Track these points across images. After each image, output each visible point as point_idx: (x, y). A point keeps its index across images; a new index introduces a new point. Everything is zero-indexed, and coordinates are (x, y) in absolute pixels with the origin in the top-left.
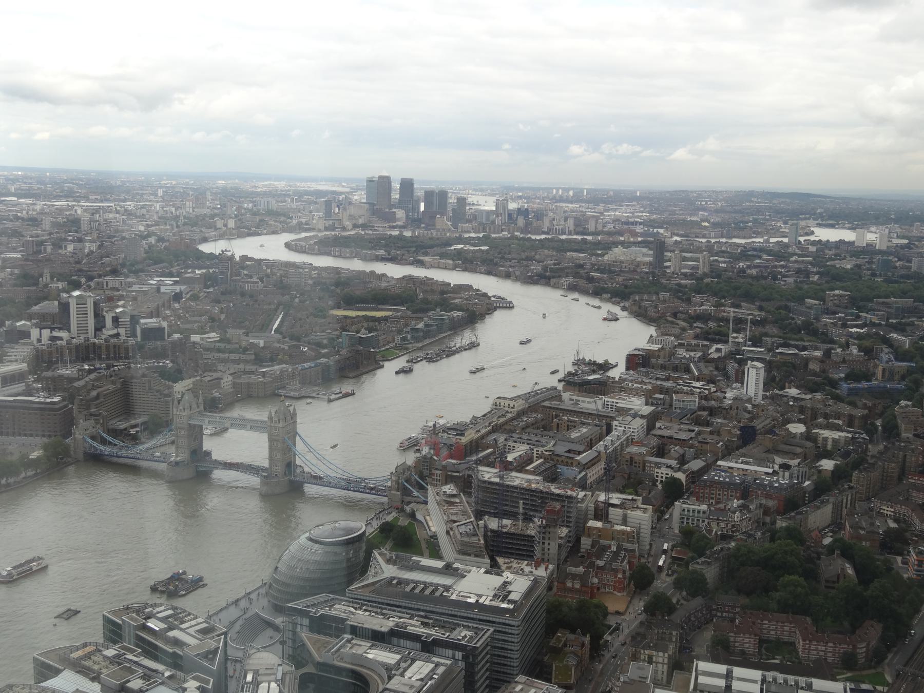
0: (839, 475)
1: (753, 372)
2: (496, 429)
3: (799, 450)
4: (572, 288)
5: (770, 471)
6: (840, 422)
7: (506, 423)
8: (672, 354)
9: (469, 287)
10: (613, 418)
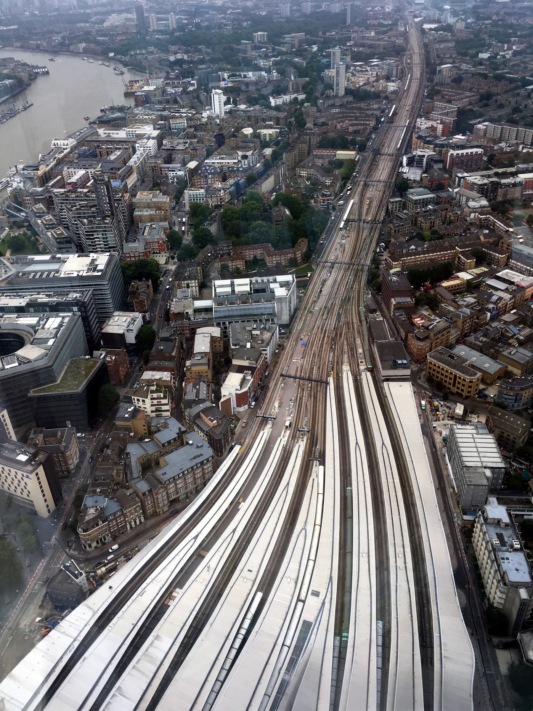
0: (276, 156)
1: (216, 97)
2: (60, 162)
4: (87, 52)
5: (236, 161)
6: (272, 123)
7: (65, 156)
8: (164, 92)
9: (13, 59)
10: (135, 142)
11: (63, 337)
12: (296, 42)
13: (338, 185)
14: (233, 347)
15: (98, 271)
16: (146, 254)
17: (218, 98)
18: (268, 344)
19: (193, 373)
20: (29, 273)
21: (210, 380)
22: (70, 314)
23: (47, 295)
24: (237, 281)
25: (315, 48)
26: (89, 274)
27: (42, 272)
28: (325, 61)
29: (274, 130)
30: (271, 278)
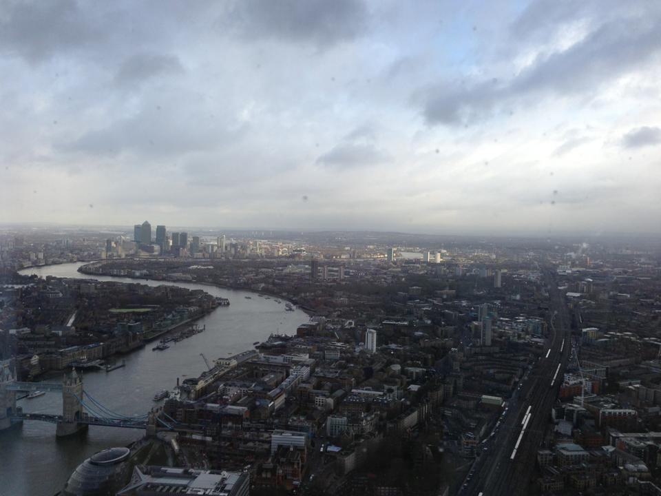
1: (370, 335)
2: (219, 379)
5: (382, 393)
7: (224, 374)
10: (290, 367)
29: (421, 369)
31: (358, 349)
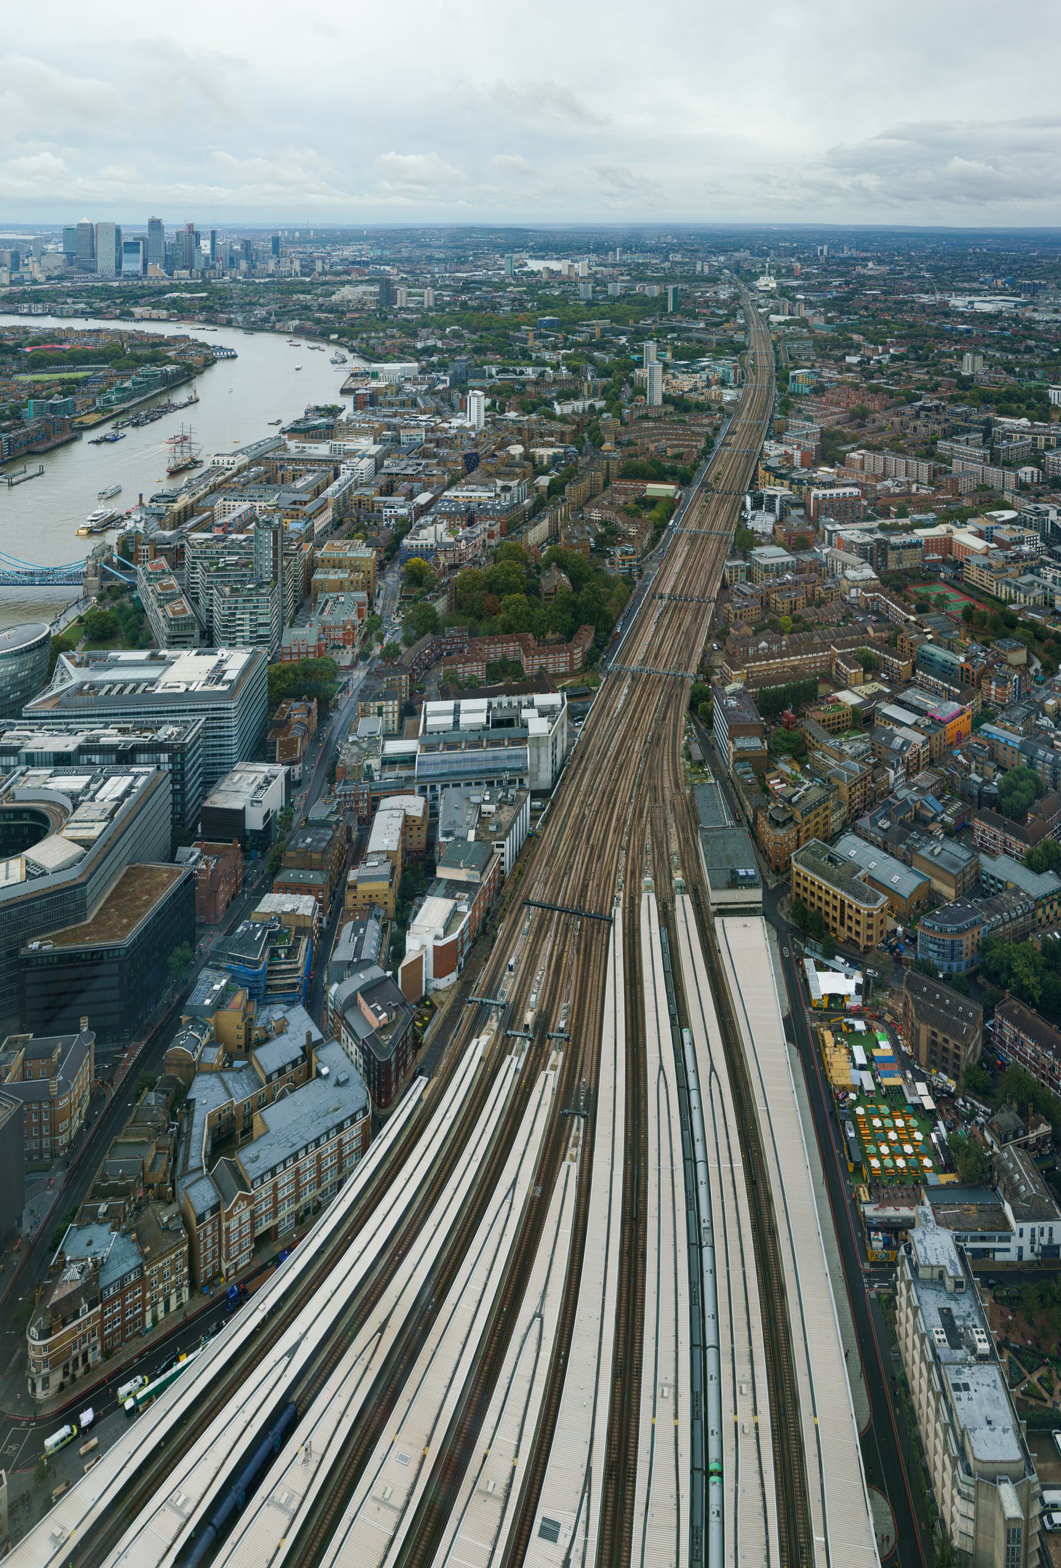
0: (555, 489)
1: (474, 400)
3: (518, 470)
6: (553, 439)
8: (400, 389)
11: (124, 820)
12: (597, 331)
13: (648, 536)
14: (442, 839)
15: (225, 683)
16: (319, 650)
17: (477, 402)
18: (507, 834)
19: (360, 897)
20: (102, 685)
21: (392, 913)
22: (151, 769)
23: (120, 730)
24: (466, 704)
25: (623, 340)
26: (206, 688)
27: (126, 684)
28: (635, 357)
29: (556, 450)
30: (524, 699)
31: (456, 422)
